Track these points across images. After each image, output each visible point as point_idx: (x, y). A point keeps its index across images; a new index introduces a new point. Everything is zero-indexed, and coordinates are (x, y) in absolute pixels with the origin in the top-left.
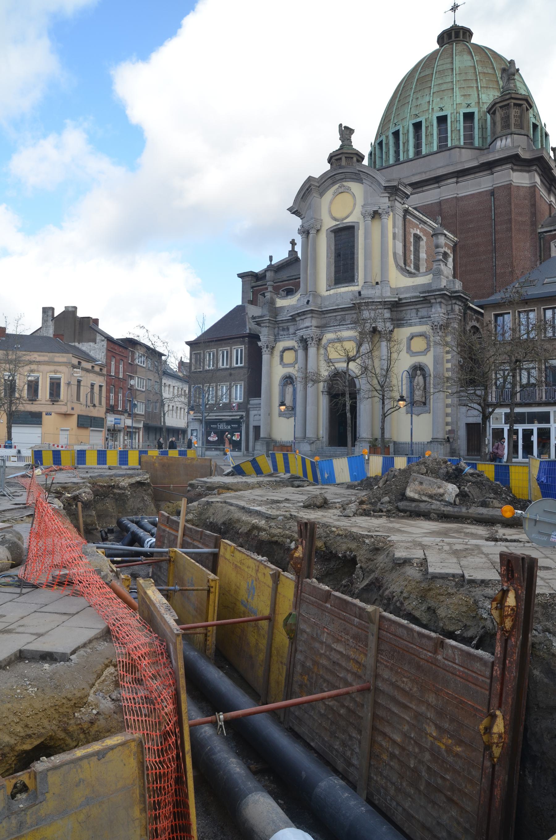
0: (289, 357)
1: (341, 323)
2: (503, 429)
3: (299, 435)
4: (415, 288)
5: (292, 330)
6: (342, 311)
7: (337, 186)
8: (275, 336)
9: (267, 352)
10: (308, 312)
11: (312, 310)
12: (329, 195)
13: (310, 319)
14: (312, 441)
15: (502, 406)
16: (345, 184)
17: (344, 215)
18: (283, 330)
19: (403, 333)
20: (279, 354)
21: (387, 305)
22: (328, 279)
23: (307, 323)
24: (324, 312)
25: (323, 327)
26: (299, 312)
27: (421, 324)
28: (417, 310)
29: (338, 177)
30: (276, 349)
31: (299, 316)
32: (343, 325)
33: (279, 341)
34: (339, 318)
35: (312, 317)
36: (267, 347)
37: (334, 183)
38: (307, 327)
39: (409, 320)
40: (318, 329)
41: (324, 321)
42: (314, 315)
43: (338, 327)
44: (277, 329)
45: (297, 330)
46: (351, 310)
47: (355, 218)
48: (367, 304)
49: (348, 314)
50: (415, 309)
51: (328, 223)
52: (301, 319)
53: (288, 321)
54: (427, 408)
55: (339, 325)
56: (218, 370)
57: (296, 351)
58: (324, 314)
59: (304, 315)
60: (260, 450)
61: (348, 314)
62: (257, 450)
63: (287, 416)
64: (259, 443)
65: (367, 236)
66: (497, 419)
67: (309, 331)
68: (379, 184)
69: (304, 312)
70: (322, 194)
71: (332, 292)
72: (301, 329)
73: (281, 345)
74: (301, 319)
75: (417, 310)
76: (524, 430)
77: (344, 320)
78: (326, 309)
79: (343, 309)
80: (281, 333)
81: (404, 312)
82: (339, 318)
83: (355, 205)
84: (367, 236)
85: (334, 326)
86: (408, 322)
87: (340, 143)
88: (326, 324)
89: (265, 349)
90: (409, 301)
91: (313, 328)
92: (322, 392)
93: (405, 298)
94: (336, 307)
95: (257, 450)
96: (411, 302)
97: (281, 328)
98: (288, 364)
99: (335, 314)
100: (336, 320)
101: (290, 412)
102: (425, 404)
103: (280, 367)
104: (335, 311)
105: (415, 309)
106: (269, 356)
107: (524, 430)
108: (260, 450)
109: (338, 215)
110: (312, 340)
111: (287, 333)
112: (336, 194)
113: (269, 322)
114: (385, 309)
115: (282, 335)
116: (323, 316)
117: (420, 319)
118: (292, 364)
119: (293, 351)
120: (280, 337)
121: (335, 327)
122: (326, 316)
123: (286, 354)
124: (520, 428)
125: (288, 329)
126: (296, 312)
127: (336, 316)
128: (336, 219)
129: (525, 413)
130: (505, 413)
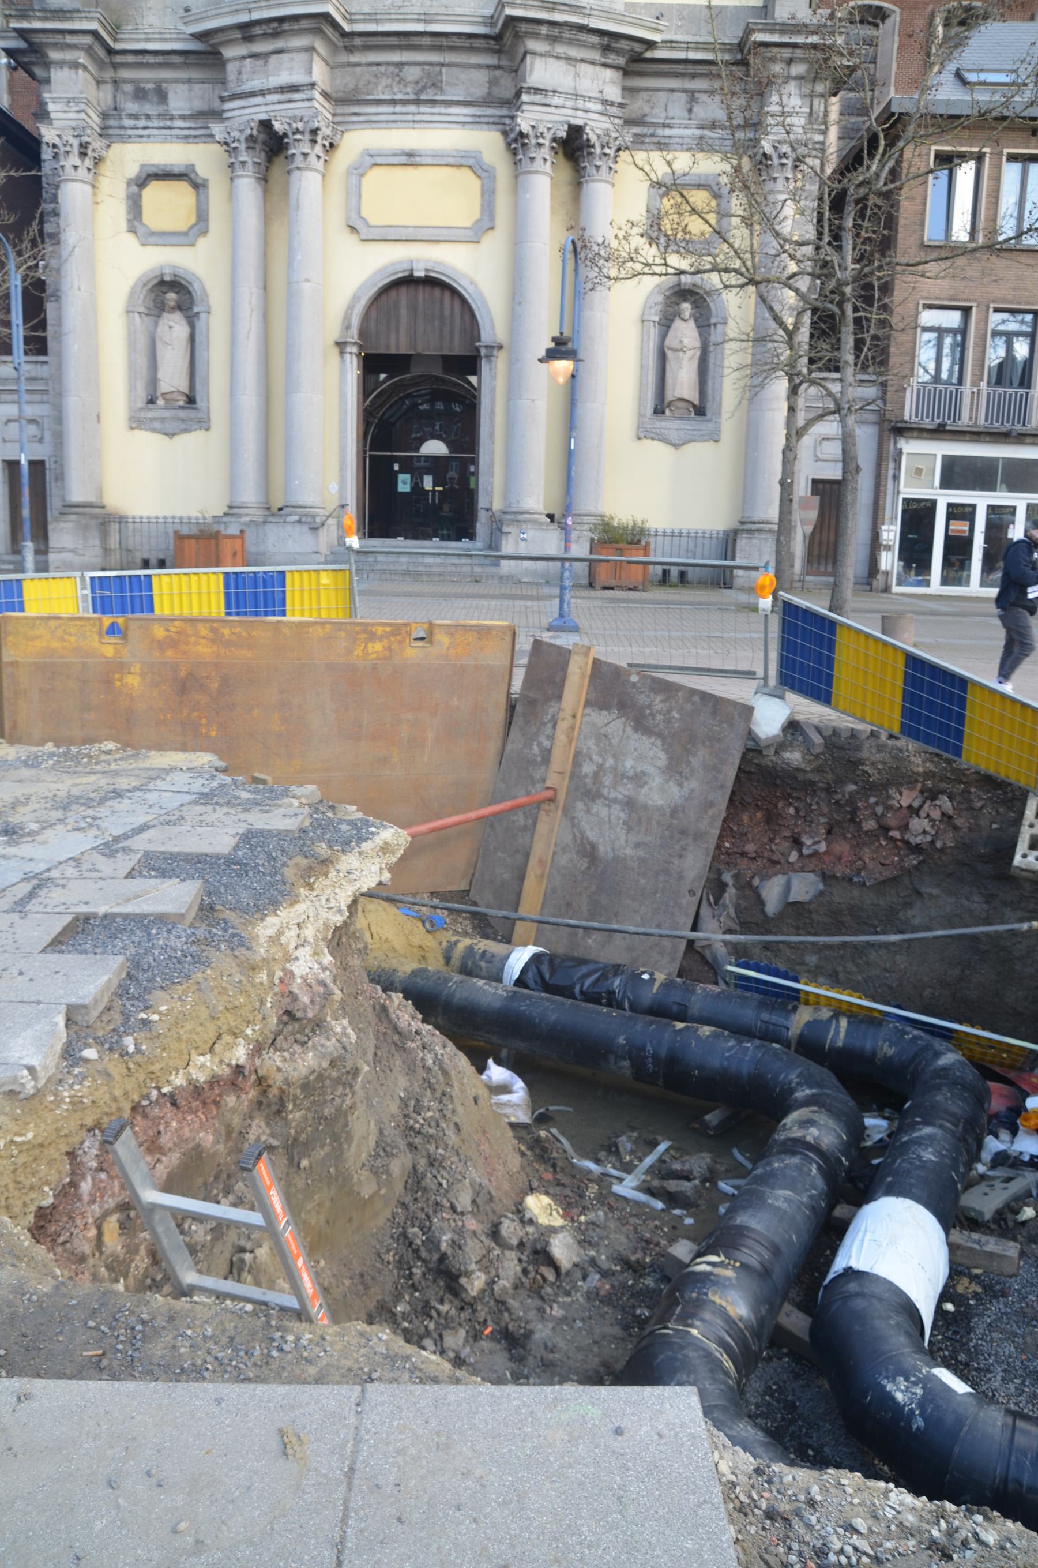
0: (168, 205)
1: (424, 97)
2: (933, 503)
3: (249, 495)
5: (182, 99)
6: (439, 48)
8: (104, 116)
9: (82, 173)
10: (305, 24)
11: (326, 17)
13: (303, 57)
14: (318, 520)
15: (939, 432)
18: (140, 94)
20: (120, 190)
21: (618, 52)
23: (286, 70)
24: (358, 41)
25: (347, 101)
26: (256, 16)
28: (692, 96)
30: (106, 169)
31: (248, 39)
32: (433, 102)
33: (124, 139)
34: (412, 74)
35: (312, 49)
36: (83, 155)
38: (293, 88)
39: (665, 126)
40: (326, 104)
41: (346, 80)
42: (319, 44)
43: (412, 108)
44: (108, 88)
45: (233, 97)
46: (471, 49)
48: (557, 32)
49: (450, 65)
50: (684, 91)
52: (253, 56)
54: (711, 426)
55: (417, 102)
57: (199, 186)
58: (350, 49)
59: (276, 35)
60: (74, 551)
61: (450, 65)
62: (61, 550)
63: (170, 427)
64: (69, 525)
66: (919, 471)
67: (298, 106)
69: (281, 20)
72: (252, 94)
73: (129, 157)
74: (253, 56)
76: (992, 509)
77: (437, 85)
78: (372, 27)
79: (441, 41)
80: (131, 107)
81: (644, 95)
82: (412, 74)
85: (393, 102)
86: (660, 132)
88: (356, 89)
89: (74, 159)
90: (681, 55)
91: (317, 95)
92: (341, 345)
93: (670, 44)
94: (420, 27)
95: (61, 550)
96: (686, 61)
97: (128, 88)
98: (163, 234)
99: (396, 57)
100: (402, 81)
101: (182, 414)
102: (700, 411)
103: (131, 239)
104: (405, 40)
105: (684, 91)
106: (88, 188)
107: (992, 509)
108: (74, 551)
110: (314, 142)
111: (161, 109)
113: (89, 50)
114: (605, 65)
115: (135, 116)
116: (344, 58)
117: (702, 127)
118: (185, 234)
119: (184, 186)
120: (127, 122)
121: (399, 108)
122: (355, 58)
123: (154, 194)
124: (981, 500)
125: (162, 96)
126: (244, 18)
127: (400, 65)
129: (997, 459)
130: (944, 457)
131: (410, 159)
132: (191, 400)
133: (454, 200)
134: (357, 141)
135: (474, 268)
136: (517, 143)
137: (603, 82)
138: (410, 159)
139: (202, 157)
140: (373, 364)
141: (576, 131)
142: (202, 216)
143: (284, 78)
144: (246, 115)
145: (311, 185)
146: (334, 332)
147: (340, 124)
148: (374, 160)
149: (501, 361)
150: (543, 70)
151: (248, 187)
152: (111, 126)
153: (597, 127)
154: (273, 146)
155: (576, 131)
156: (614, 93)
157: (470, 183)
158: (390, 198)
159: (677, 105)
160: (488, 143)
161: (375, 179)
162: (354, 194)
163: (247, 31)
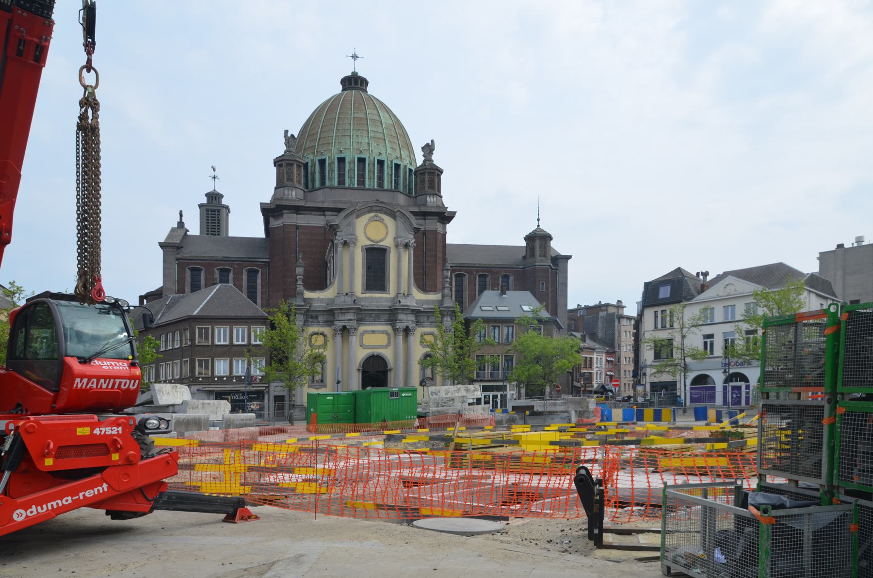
4: (428, 302)
5: (321, 319)
7: (372, 214)
12: (365, 219)
16: (380, 215)
17: (378, 238)
18: (312, 317)
19: (420, 331)
22: (363, 285)
23: (350, 316)
25: (360, 321)
27: (431, 326)
28: (428, 317)
29: (375, 208)
37: (370, 212)
41: (360, 317)
47: (388, 242)
48: (403, 309)
51: (363, 242)
53: (319, 311)
56: (231, 345)
65: (399, 261)
67: (352, 323)
68: (411, 224)
70: (357, 217)
71: (367, 295)
75: (428, 317)
79: (379, 310)
83: (387, 233)
84: (399, 261)
87: (285, 148)
92: (359, 370)
109: (372, 238)
112: (371, 220)
128: (371, 241)
131: (373, 332)
132: (322, 381)
133: (382, 339)
134: (362, 328)
135: (387, 353)
136: (396, 330)
137: (412, 317)
138: (373, 332)
139: (327, 330)
140: (363, 373)
141: (407, 327)
142: (326, 342)
143: (349, 318)
144: (339, 324)
145: (354, 339)
146: (357, 367)
147: (359, 325)
148: (365, 332)
149: (392, 372)
150: (401, 316)
151: (339, 338)
152: (306, 323)
153: (411, 325)
154: (345, 331)
155: (407, 327)
156: (414, 319)
157: (385, 337)
158: (369, 340)
159: (425, 319)
160: (389, 329)
161: (366, 337)
162: (361, 339)
163: (341, 309)
